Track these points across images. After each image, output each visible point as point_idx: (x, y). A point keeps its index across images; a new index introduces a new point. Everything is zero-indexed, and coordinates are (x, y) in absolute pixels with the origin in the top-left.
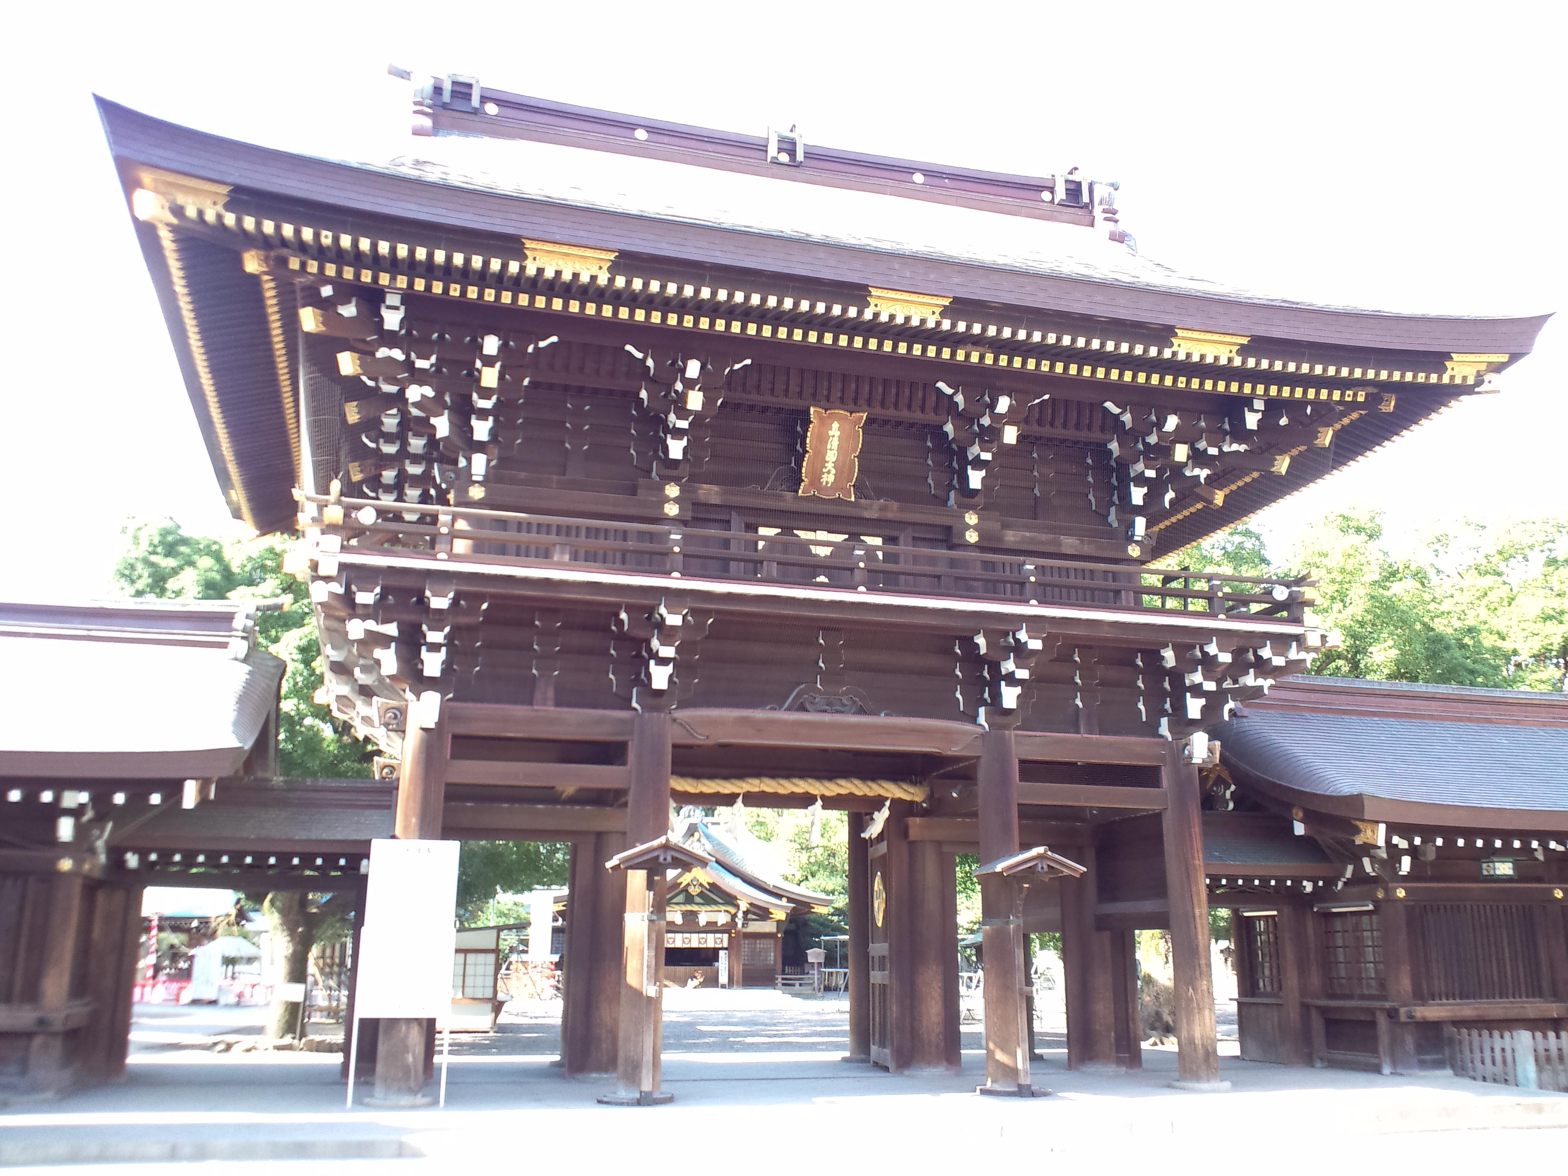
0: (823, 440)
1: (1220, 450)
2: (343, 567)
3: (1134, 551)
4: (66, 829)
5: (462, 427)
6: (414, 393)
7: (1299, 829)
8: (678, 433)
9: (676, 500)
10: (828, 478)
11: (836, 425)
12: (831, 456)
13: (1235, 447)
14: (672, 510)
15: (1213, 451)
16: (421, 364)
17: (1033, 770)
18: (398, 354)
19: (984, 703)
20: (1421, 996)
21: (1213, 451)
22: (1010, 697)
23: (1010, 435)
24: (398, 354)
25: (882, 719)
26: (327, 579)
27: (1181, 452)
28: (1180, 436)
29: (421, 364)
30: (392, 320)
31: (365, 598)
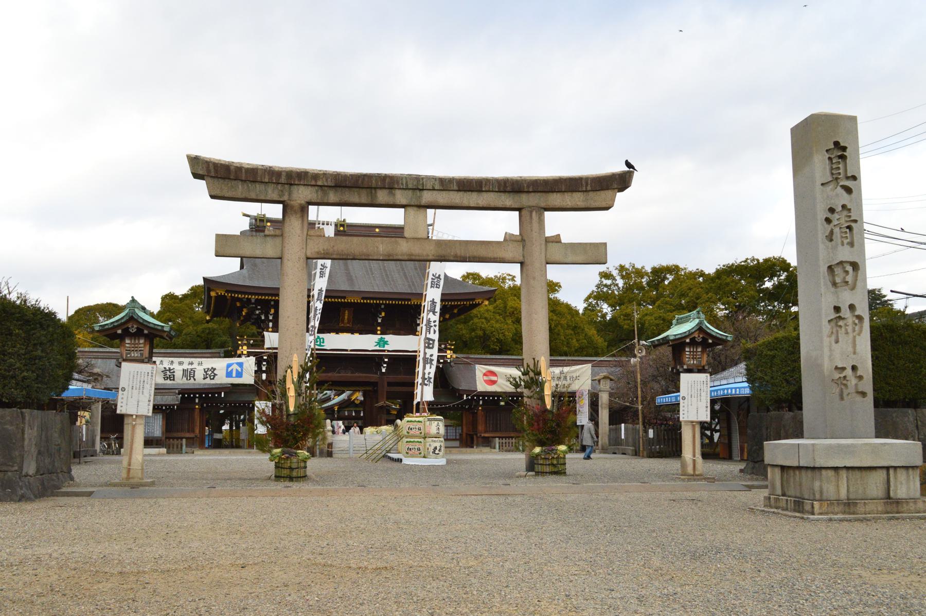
0: (344, 314)
4: (197, 401)
5: (267, 317)
6: (257, 312)
10: (346, 321)
17: (390, 384)
20: (486, 432)
22: (384, 370)
25: (357, 374)
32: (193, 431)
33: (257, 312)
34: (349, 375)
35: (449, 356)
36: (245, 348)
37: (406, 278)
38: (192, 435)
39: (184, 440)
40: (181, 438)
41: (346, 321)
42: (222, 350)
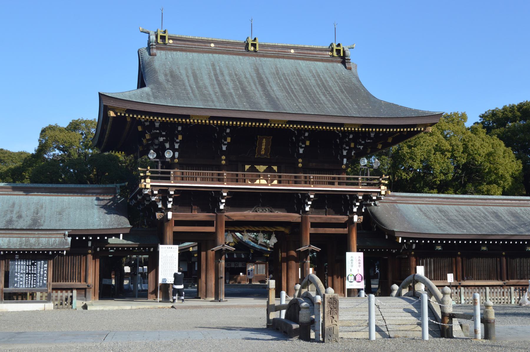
1: (365, 142)
2: (151, 186)
3: (344, 167)
4: (90, 244)
6: (161, 139)
7: (387, 237)
8: (225, 144)
9: (224, 160)
10: (263, 152)
11: (264, 139)
12: (263, 147)
13: (369, 141)
14: (223, 162)
15: (363, 142)
16: (164, 133)
17: (314, 225)
18: (158, 131)
19: (302, 209)
21: (363, 142)
23: (308, 143)
24: (158, 131)
26: (148, 189)
27: (352, 145)
28: (353, 140)
29: (164, 133)
30: (157, 125)
31: (156, 192)
32: (86, 281)
33: (161, 139)
34: (268, 213)
35: (383, 193)
36: (148, 180)
37: (335, 102)
38: (82, 285)
39: (75, 292)
40: (71, 290)
41: (263, 152)
42: (118, 185)
